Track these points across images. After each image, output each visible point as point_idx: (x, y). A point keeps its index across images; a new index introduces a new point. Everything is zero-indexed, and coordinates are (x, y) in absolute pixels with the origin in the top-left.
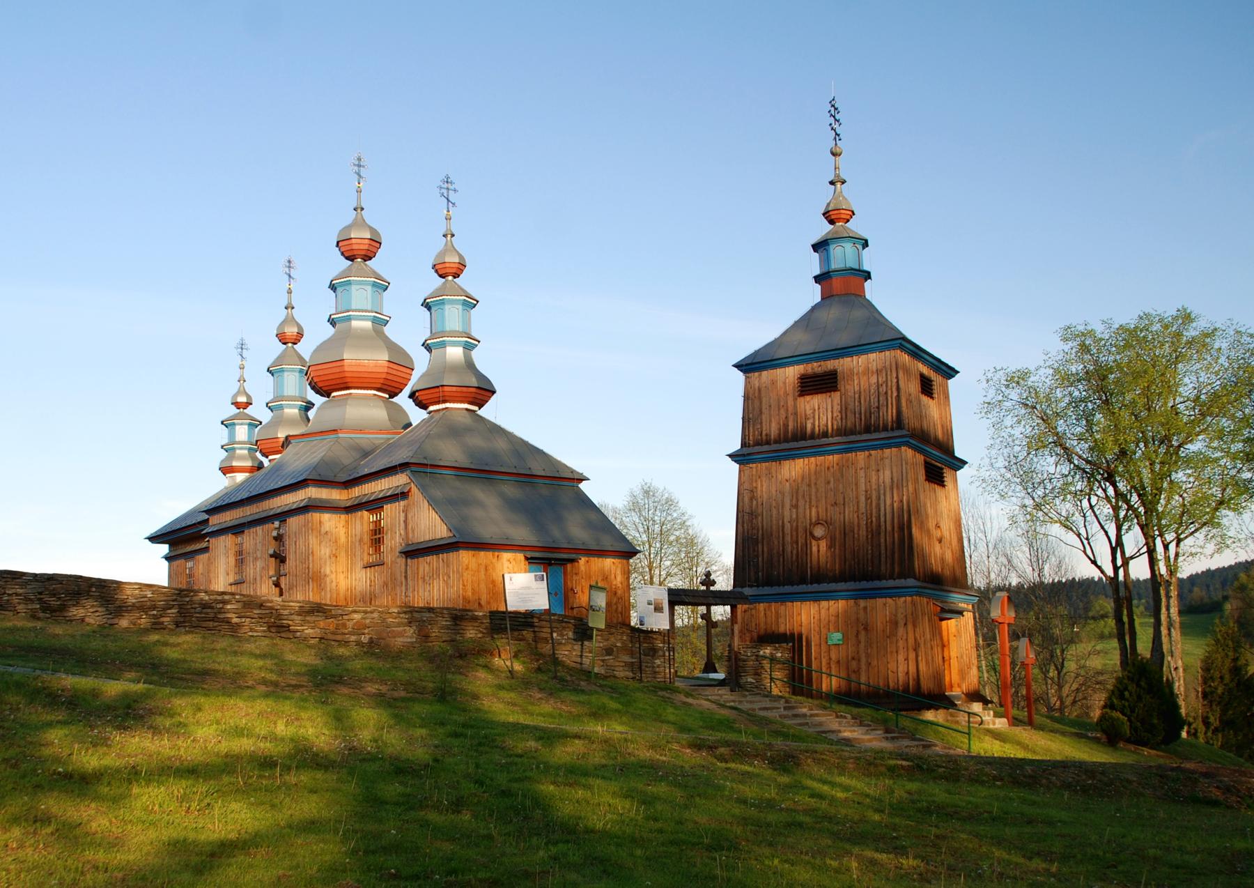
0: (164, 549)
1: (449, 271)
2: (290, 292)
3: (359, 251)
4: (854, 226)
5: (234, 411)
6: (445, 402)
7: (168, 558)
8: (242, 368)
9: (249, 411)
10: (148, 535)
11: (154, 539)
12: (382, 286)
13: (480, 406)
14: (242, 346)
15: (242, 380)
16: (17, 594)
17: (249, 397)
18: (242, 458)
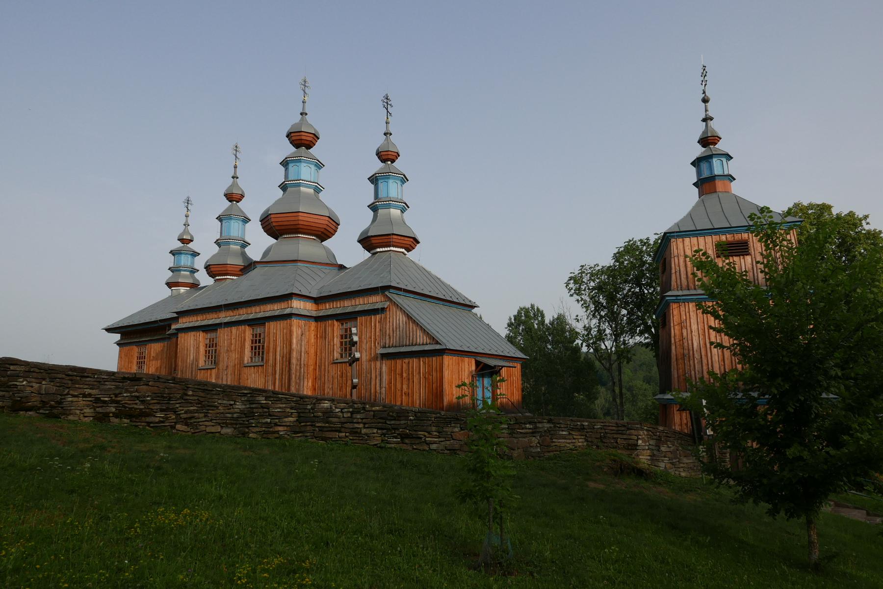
0: (117, 337)
1: (386, 156)
2: (235, 167)
3: (302, 140)
4: (721, 146)
5: (179, 244)
6: (390, 246)
7: (118, 344)
8: (187, 216)
9: (191, 245)
10: (105, 326)
11: (109, 330)
12: (319, 165)
13: (408, 250)
14: (188, 201)
15: (186, 225)
16: (84, 396)
17: (192, 236)
18: (185, 277)
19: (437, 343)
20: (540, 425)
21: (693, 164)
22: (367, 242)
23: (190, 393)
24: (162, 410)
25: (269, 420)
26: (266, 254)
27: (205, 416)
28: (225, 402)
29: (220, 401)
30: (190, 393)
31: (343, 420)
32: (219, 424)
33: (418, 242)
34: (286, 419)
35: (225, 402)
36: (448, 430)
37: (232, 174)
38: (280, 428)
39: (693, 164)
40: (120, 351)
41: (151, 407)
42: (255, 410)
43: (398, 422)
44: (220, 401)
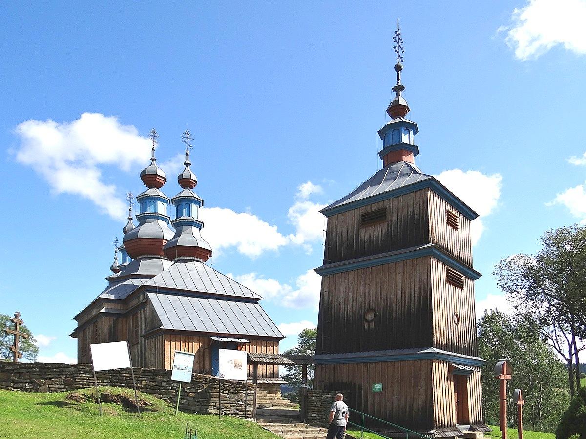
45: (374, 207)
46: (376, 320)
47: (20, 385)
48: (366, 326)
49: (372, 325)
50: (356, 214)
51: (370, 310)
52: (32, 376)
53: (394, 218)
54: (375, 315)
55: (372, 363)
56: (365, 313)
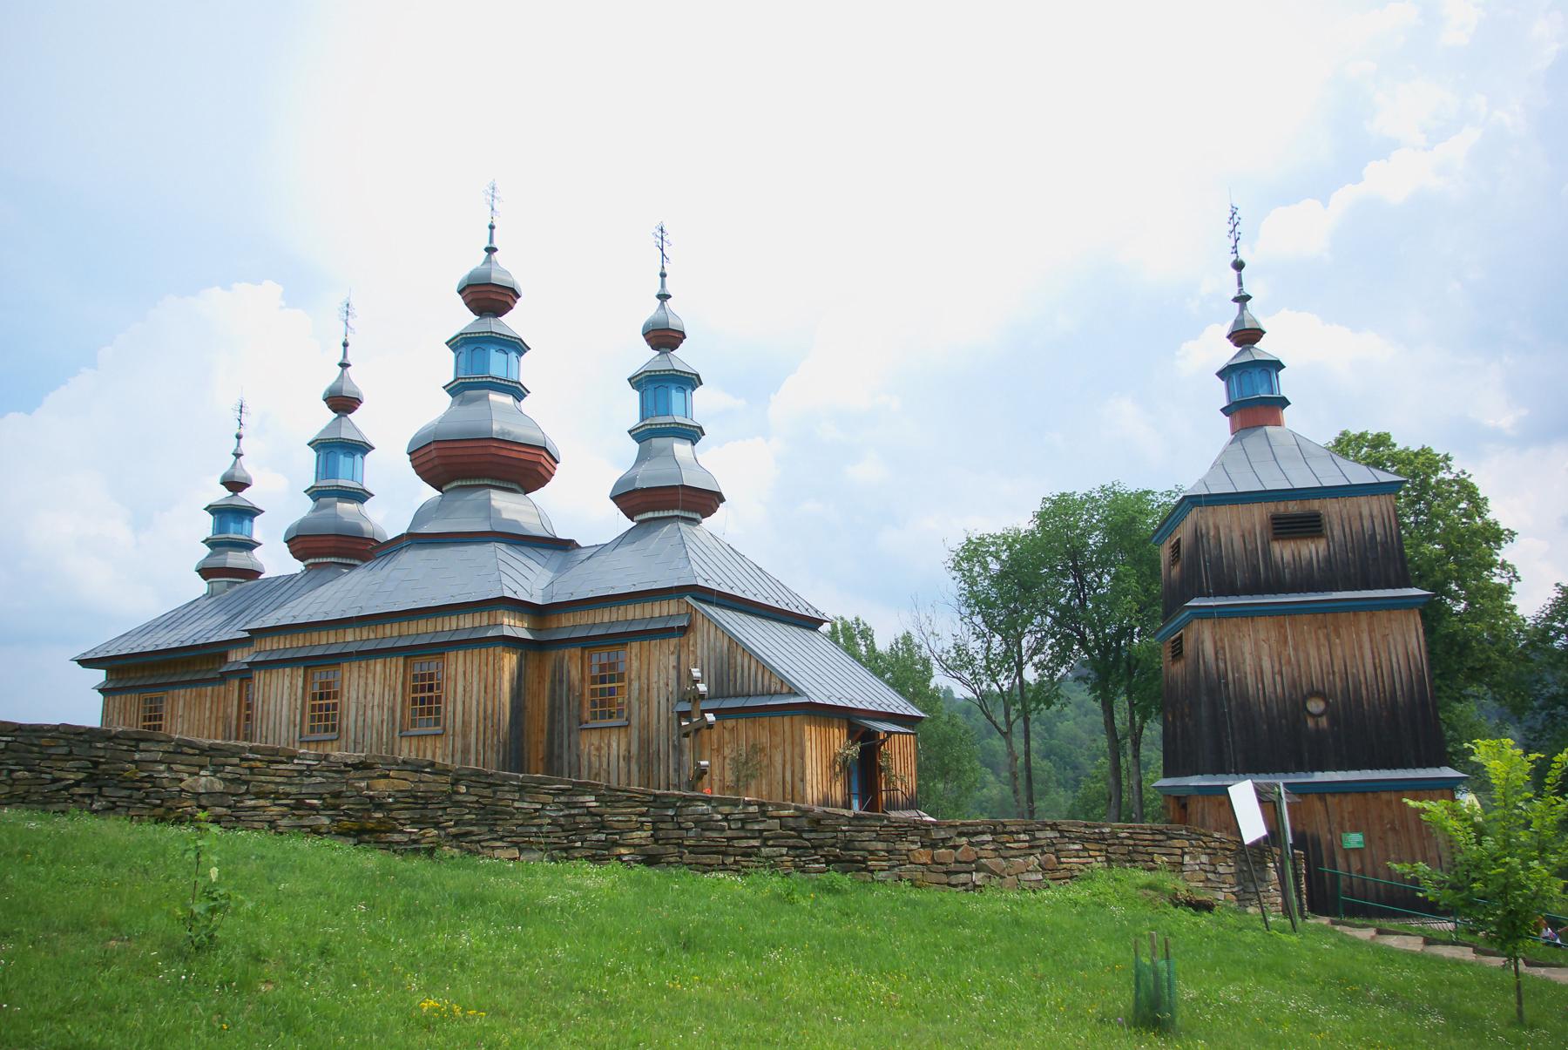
0: (100, 676)
5: (225, 493)
11: (86, 663)
19: (794, 692)
20: (1038, 834)
21: (1222, 374)
22: (629, 499)
23: (463, 789)
24: (414, 822)
25: (603, 837)
26: (421, 515)
27: (491, 831)
28: (525, 805)
29: (516, 804)
30: (463, 789)
31: (729, 833)
32: (516, 844)
33: (722, 500)
34: (635, 834)
35: (525, 805)
36: (903, 846)
37: (340, 359)
38: (623, 851)
39: (1222, 374)
40: (106, 705)
41: (394, 814)
42: (578, 819)
43: (821, 836)
44: (516, 804)
45: (1293, 507)
46: (1329, 711)
47: (963, 878)
48: (1310, 723)
49: (1324, 722)
50: (1258, 515)
51: (1314, 694)
52: (982, 853)
53: (1337, 532)
54: (1327, 703)
55: (1333, 794)
56: (1305, 699)
